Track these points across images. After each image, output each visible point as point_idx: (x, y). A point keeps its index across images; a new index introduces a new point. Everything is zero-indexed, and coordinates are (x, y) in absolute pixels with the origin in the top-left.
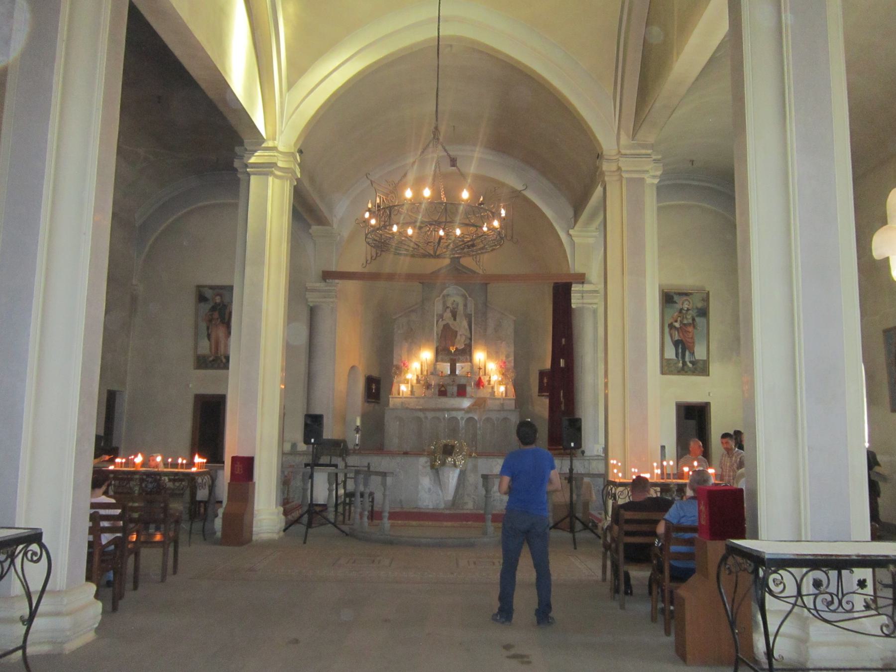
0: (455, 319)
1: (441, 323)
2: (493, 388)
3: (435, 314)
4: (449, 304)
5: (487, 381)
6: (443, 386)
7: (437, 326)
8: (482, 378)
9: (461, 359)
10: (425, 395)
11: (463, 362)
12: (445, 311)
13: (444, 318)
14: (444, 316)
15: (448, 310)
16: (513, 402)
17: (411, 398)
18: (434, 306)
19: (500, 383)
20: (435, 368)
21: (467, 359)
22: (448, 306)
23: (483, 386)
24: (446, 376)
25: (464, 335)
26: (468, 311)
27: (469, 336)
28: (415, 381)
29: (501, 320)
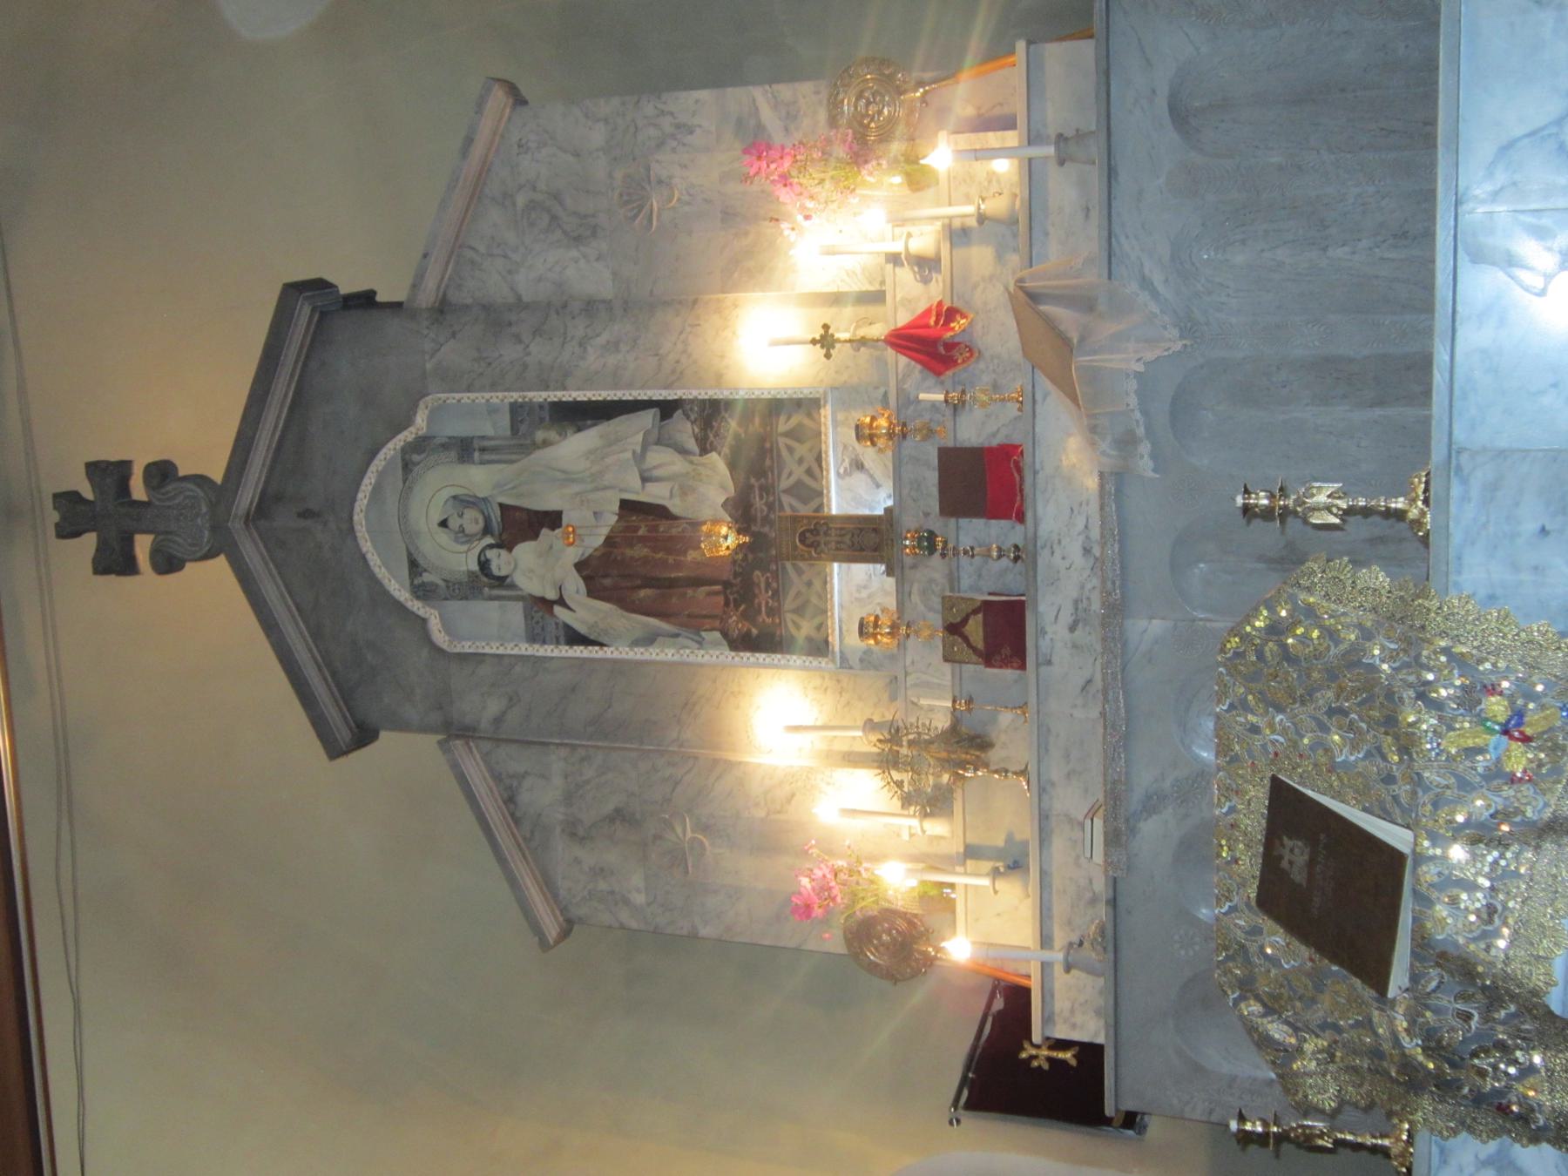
0: (553, 519)
1: (584, 612)
2: (957, 235)
3: (525, 649)
4: (464, 561)
5: (926, 281)
6: (954, 629)
7: (602, 645)
8: (903, 319)
9: (799, 473)
10: (1023, 773)
11: (819, 459)
12: (501, 581)
13: (551, 595)
14: (537, 592)
15: (500, 562)
16: (1055, 53)
17: (1044, 874)
18: (479, 658)
19: (918, 179)
20: (867, 662)
21: (794, 434)
22: (475, 567)
23: (951, 314)
24: (902, 595)
25: (639, 458)
26: (495, 428)
27: (648, 418)
28: (937, 827)
29: (521, 200)
